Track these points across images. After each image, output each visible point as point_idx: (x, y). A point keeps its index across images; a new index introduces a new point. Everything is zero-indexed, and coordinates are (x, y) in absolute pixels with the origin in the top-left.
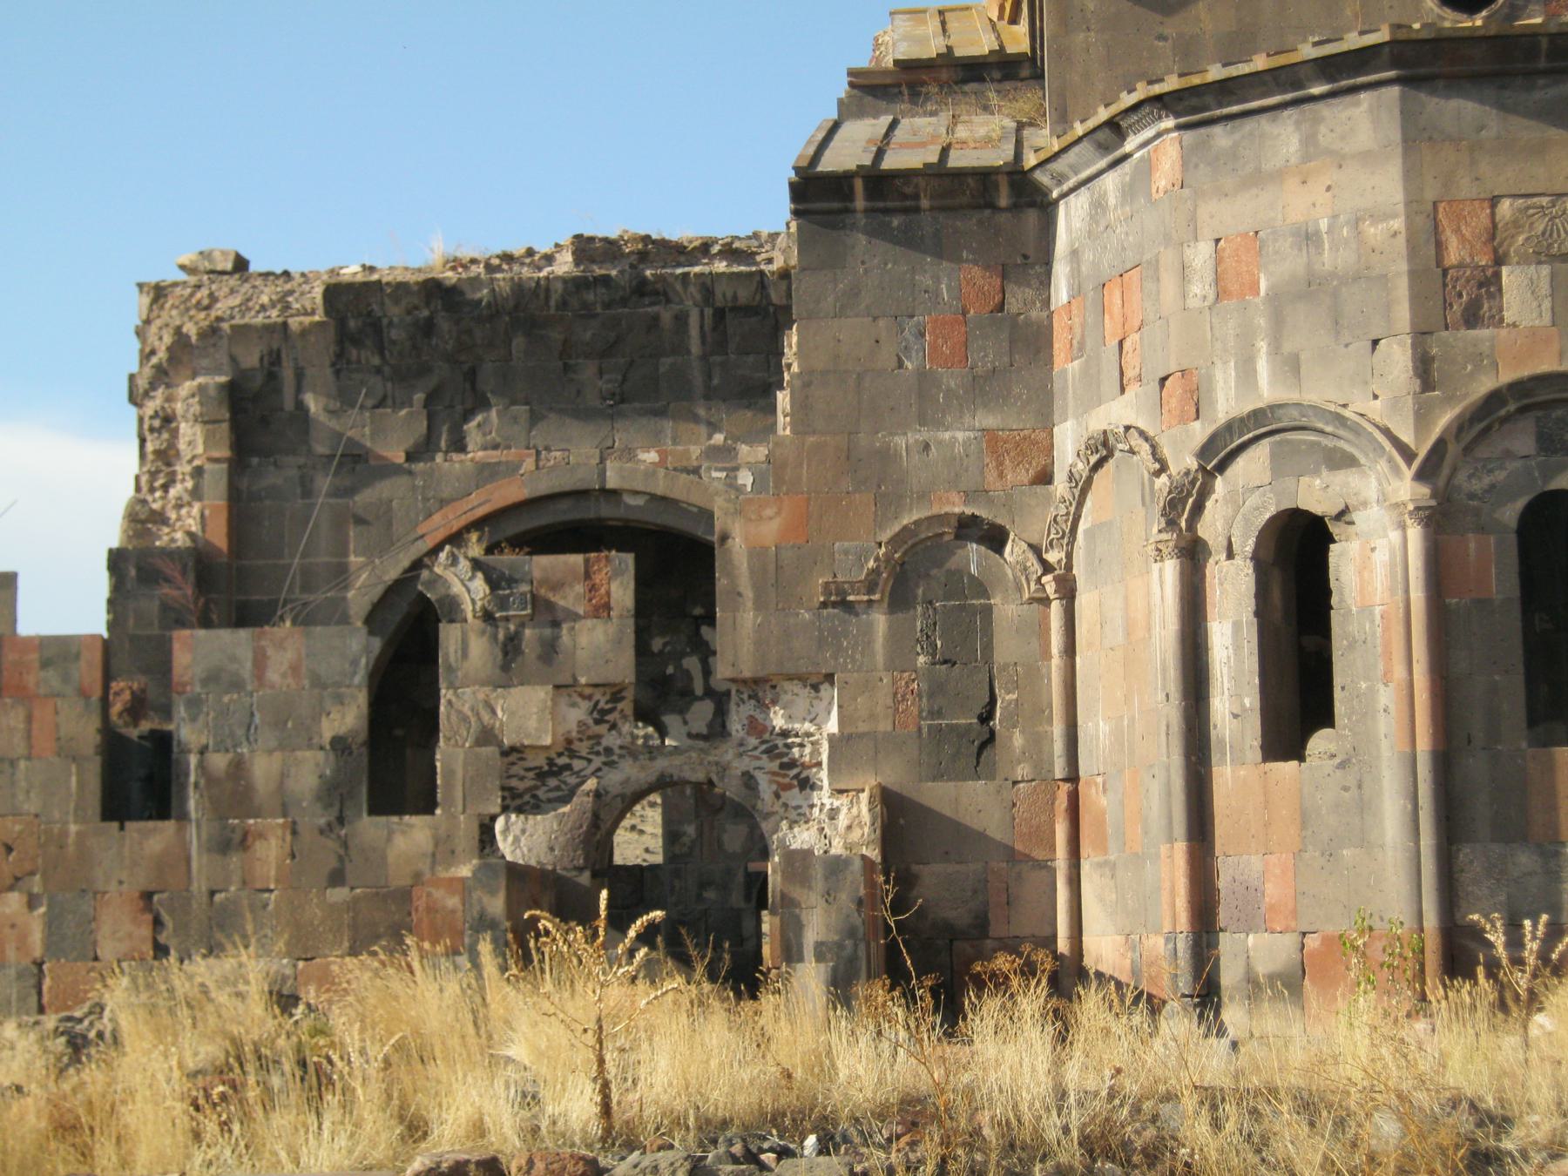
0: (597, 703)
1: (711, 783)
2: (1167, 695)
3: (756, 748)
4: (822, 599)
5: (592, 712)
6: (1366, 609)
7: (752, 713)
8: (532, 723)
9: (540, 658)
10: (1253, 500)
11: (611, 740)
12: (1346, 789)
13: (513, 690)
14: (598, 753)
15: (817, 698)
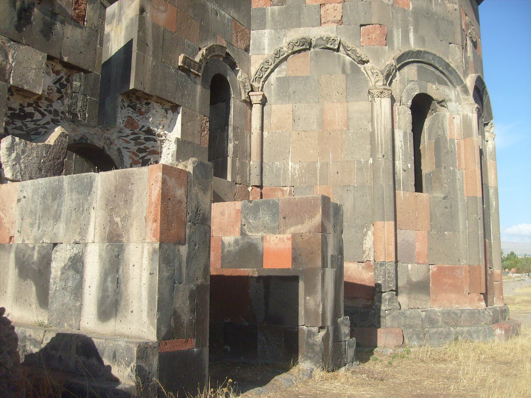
0: (62, 77)
1: (103, 147)
2: (383, 156)
3: (127, 136)
4: (180, 64)
5: (55, 83)
6: (452, 140)
7: (130, 115)
8: (32, 75)
9: (42, 31)
10: (410, 85)
11: (57, 106)
12: (446, 208)
13: (22, 47)
14: (50, 112)
15: (166, 117)
